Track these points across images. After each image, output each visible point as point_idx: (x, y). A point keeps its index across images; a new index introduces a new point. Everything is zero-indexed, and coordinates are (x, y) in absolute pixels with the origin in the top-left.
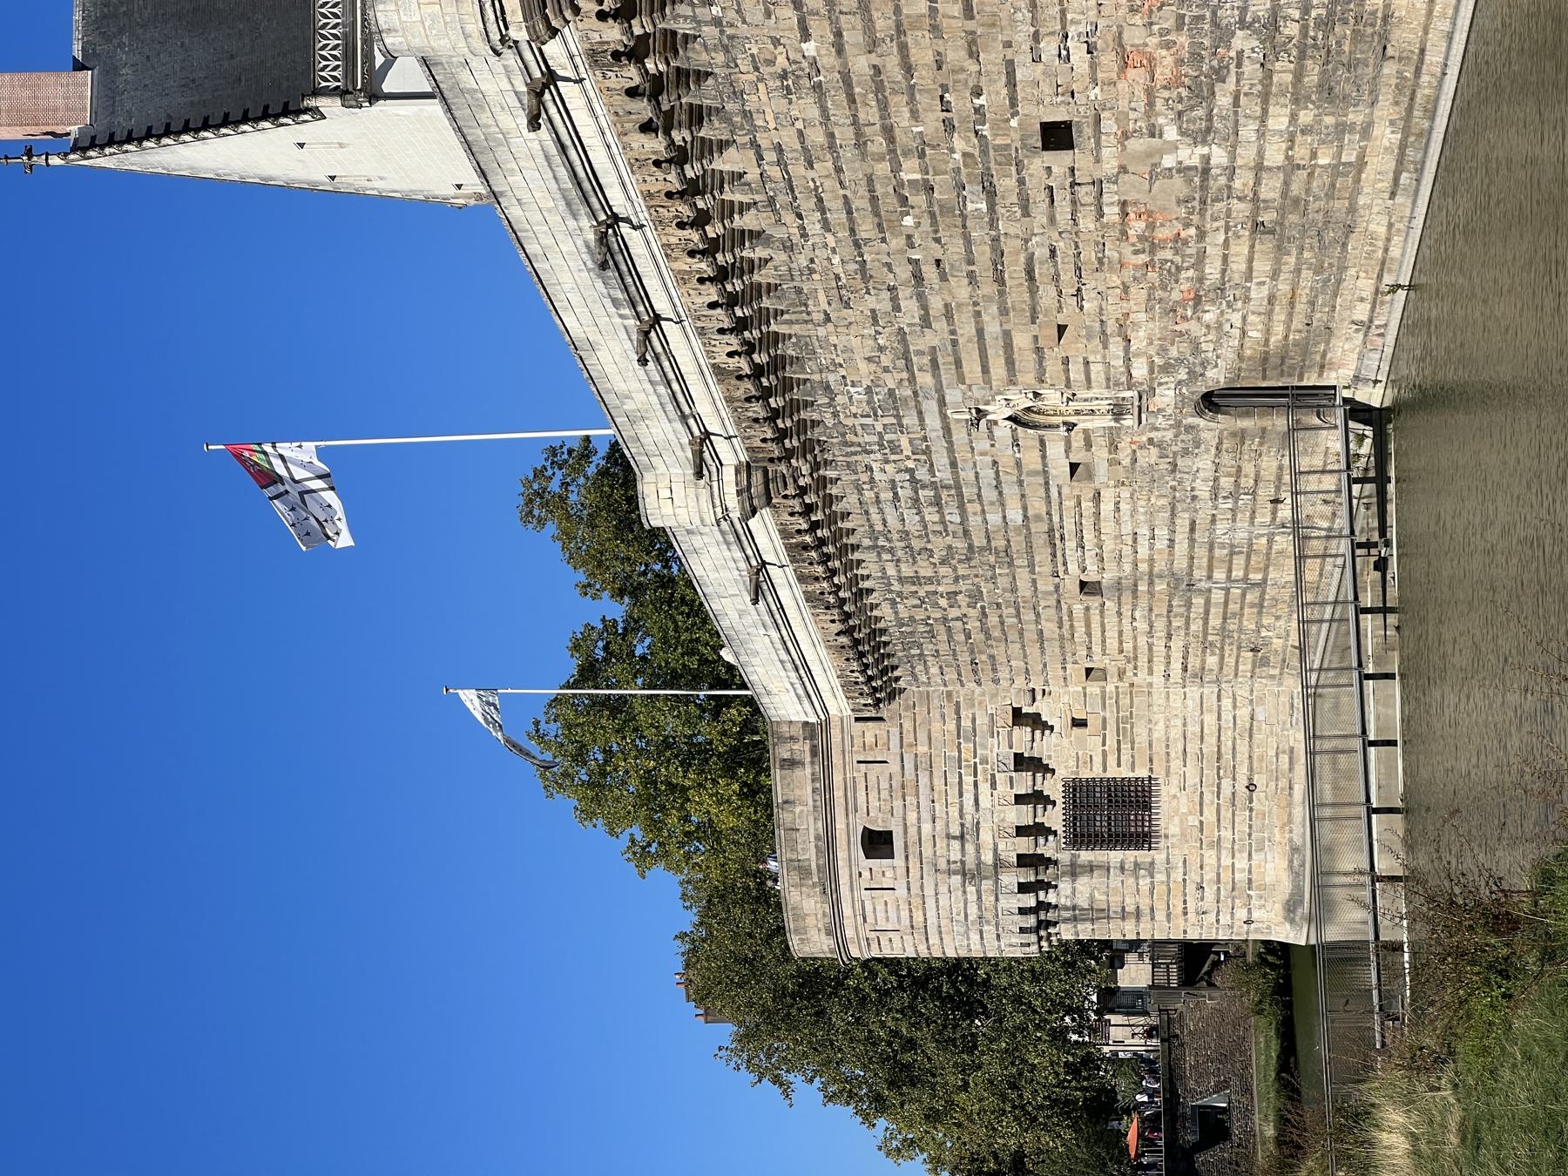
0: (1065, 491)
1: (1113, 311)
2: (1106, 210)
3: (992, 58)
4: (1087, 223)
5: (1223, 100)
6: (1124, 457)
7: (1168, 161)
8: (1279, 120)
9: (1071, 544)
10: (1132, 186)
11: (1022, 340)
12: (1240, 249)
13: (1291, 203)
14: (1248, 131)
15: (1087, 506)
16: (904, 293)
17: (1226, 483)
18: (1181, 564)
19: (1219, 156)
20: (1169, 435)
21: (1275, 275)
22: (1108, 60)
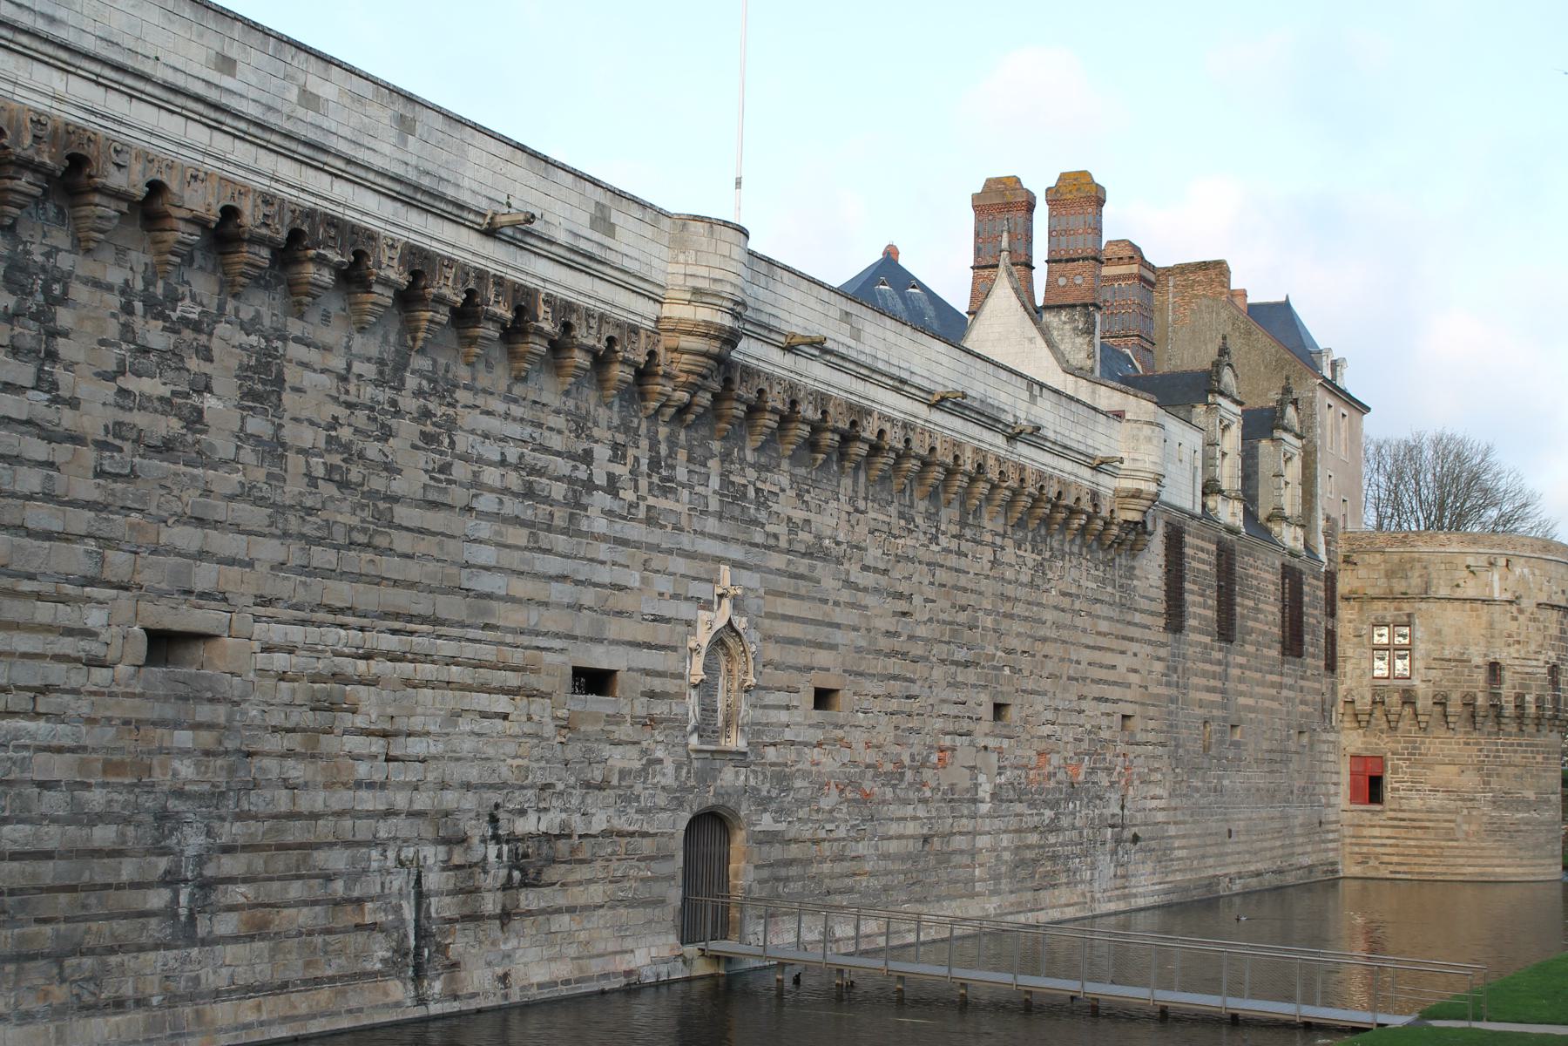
0: (548, 657)
1: (858, 737)
2: (948, 737)
3: (1047, 684)
4: (939, 724)
5: (1019, 808)
6: (624, 731)
7: (982, 778)
8: (1006, 840)
10: (965, 755)
11: (823, 657)
12: (911, 828)
13: (944, 858)
14: (998, 824)
16: (883, 581)
19: (984, 808)
20: (669, 781)
22: (1042, 746)
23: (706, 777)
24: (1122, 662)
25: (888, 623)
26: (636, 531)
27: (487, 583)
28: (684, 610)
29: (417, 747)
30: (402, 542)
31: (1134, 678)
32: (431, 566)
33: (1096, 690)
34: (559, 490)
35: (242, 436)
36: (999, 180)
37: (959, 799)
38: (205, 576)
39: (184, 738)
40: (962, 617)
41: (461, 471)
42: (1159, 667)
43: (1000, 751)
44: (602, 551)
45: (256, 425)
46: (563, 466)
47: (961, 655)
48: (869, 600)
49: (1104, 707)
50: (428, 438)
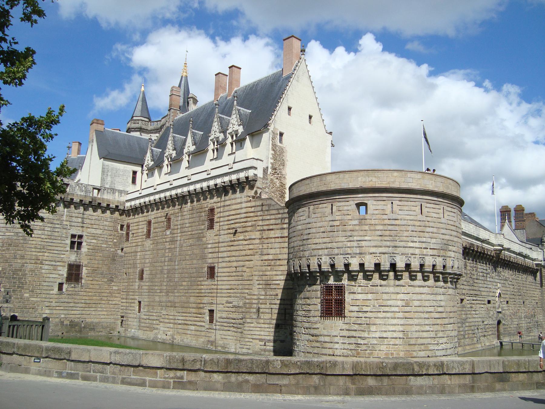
0: (486, 299)
1: (510, 308)
3: (528, 298)
5: (526, 319)
6: (492, 309)
9: (475, 298)
10: (521, 311)
11: (507, 296)
15: (483, 302)
17: (487, 326)
18: (469, 320)
19: (523, 319)
21: (514, 327)
23: (498, 316)
24: (536, 293)
25: (512, 290)
26: (491, 280)
27: (481, 289)
28: (495, 290)
29: (477, 312)
30: (475, 285)
31: (537, 296)
32: (477, 288)
33: (534, 298)
34: (485, 275)
35: (465, 273)
36: (504, 206)
37: (520, 318)
38: (464, 292)
39: (463, 312)
40: (519, 288)
41: (478, 274)
42: (540, 293)
43: (524, 310)
44: (489, 283)
45: (466, 272)
46: (485, 271)
47: (519, 294)
48: (511, 286)
49: (534, 301)
50: (476, 270)
